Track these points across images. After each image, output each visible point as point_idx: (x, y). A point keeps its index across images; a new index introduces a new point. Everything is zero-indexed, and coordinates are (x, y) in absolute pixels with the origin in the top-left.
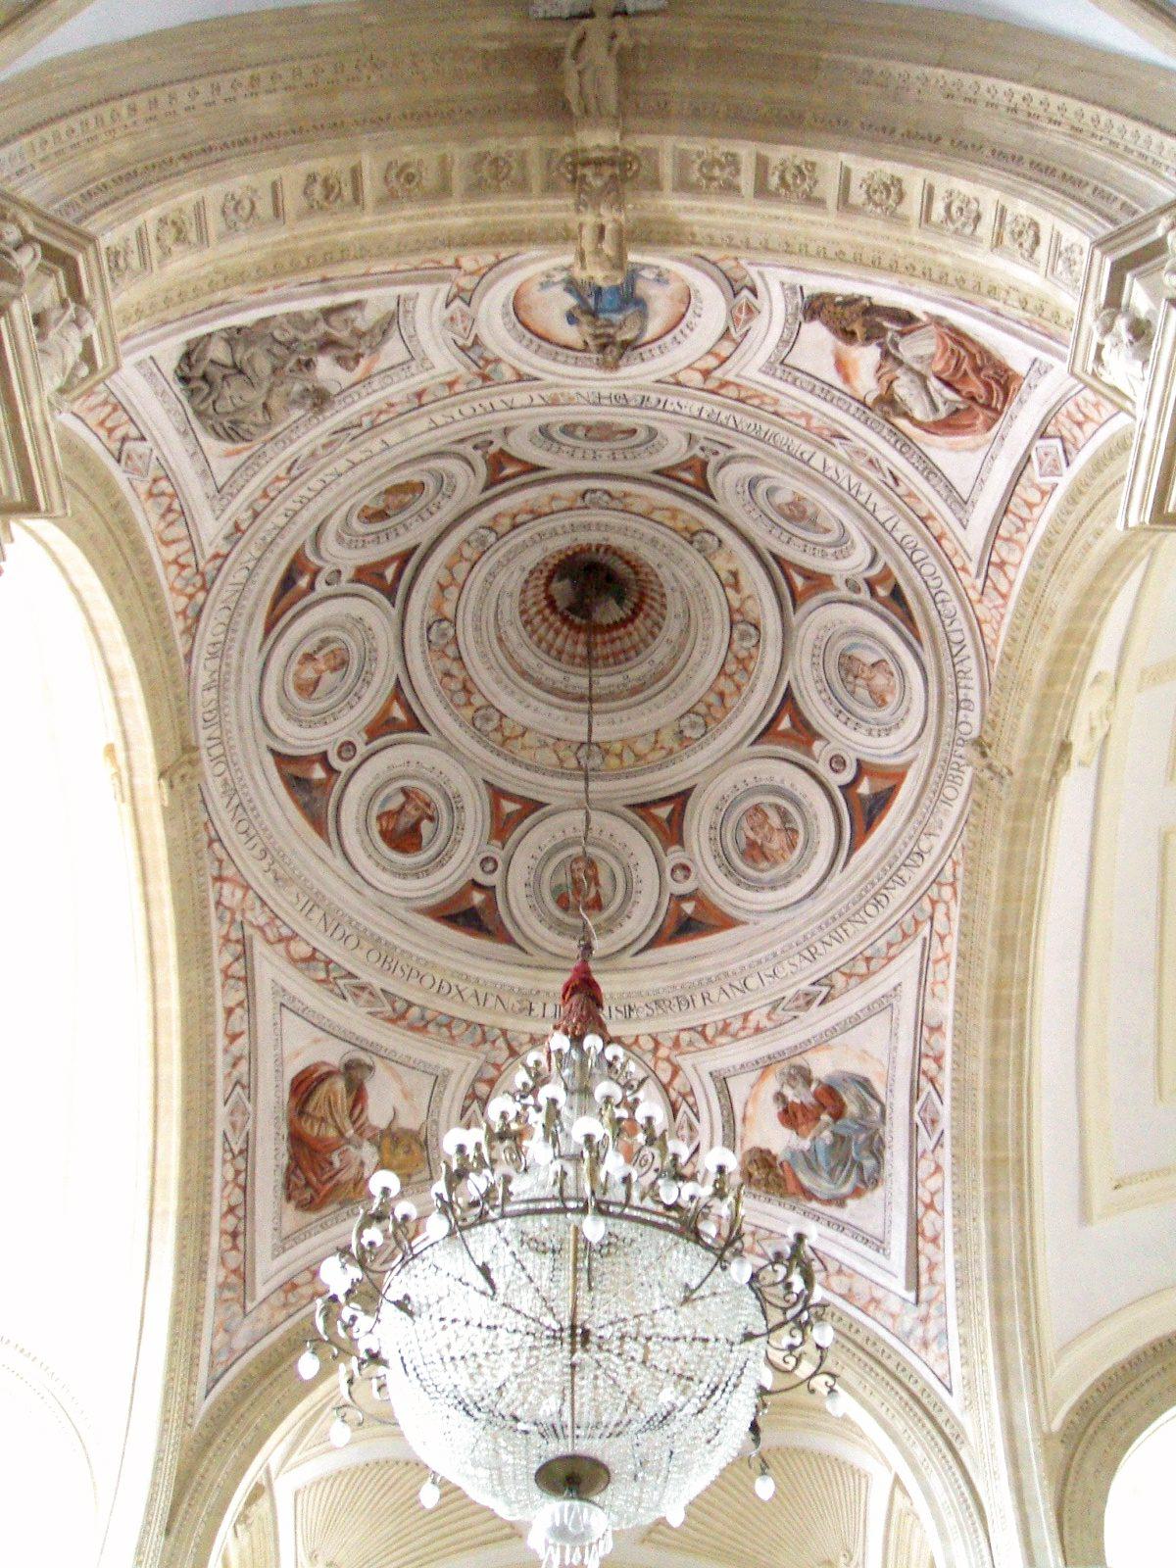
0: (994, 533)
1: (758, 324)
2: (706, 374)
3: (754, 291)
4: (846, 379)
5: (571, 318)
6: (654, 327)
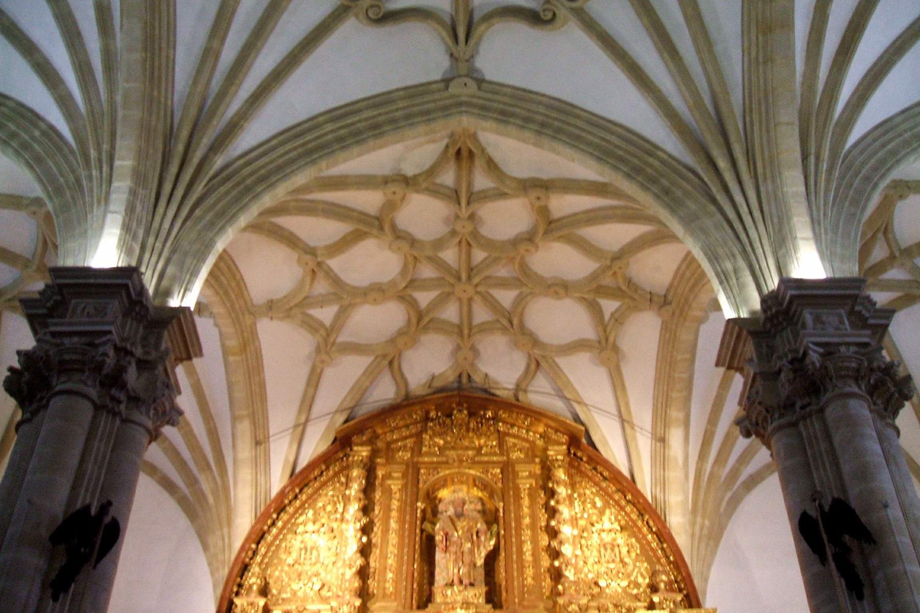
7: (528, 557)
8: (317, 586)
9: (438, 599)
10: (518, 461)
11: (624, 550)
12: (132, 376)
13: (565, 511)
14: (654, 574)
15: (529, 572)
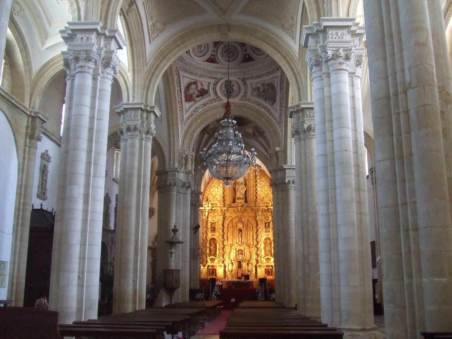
0: (179, 77)
1: (213, 87)
2: (217, 79)
3: (214, 92)
4: (201, 83)
5: (233, 85)
6: (224, 83)
8: (216, 199)
9: (236, 202)
11: (269, 191)
12: (197, 205)
13: (258, 185)
15: (252, 196)
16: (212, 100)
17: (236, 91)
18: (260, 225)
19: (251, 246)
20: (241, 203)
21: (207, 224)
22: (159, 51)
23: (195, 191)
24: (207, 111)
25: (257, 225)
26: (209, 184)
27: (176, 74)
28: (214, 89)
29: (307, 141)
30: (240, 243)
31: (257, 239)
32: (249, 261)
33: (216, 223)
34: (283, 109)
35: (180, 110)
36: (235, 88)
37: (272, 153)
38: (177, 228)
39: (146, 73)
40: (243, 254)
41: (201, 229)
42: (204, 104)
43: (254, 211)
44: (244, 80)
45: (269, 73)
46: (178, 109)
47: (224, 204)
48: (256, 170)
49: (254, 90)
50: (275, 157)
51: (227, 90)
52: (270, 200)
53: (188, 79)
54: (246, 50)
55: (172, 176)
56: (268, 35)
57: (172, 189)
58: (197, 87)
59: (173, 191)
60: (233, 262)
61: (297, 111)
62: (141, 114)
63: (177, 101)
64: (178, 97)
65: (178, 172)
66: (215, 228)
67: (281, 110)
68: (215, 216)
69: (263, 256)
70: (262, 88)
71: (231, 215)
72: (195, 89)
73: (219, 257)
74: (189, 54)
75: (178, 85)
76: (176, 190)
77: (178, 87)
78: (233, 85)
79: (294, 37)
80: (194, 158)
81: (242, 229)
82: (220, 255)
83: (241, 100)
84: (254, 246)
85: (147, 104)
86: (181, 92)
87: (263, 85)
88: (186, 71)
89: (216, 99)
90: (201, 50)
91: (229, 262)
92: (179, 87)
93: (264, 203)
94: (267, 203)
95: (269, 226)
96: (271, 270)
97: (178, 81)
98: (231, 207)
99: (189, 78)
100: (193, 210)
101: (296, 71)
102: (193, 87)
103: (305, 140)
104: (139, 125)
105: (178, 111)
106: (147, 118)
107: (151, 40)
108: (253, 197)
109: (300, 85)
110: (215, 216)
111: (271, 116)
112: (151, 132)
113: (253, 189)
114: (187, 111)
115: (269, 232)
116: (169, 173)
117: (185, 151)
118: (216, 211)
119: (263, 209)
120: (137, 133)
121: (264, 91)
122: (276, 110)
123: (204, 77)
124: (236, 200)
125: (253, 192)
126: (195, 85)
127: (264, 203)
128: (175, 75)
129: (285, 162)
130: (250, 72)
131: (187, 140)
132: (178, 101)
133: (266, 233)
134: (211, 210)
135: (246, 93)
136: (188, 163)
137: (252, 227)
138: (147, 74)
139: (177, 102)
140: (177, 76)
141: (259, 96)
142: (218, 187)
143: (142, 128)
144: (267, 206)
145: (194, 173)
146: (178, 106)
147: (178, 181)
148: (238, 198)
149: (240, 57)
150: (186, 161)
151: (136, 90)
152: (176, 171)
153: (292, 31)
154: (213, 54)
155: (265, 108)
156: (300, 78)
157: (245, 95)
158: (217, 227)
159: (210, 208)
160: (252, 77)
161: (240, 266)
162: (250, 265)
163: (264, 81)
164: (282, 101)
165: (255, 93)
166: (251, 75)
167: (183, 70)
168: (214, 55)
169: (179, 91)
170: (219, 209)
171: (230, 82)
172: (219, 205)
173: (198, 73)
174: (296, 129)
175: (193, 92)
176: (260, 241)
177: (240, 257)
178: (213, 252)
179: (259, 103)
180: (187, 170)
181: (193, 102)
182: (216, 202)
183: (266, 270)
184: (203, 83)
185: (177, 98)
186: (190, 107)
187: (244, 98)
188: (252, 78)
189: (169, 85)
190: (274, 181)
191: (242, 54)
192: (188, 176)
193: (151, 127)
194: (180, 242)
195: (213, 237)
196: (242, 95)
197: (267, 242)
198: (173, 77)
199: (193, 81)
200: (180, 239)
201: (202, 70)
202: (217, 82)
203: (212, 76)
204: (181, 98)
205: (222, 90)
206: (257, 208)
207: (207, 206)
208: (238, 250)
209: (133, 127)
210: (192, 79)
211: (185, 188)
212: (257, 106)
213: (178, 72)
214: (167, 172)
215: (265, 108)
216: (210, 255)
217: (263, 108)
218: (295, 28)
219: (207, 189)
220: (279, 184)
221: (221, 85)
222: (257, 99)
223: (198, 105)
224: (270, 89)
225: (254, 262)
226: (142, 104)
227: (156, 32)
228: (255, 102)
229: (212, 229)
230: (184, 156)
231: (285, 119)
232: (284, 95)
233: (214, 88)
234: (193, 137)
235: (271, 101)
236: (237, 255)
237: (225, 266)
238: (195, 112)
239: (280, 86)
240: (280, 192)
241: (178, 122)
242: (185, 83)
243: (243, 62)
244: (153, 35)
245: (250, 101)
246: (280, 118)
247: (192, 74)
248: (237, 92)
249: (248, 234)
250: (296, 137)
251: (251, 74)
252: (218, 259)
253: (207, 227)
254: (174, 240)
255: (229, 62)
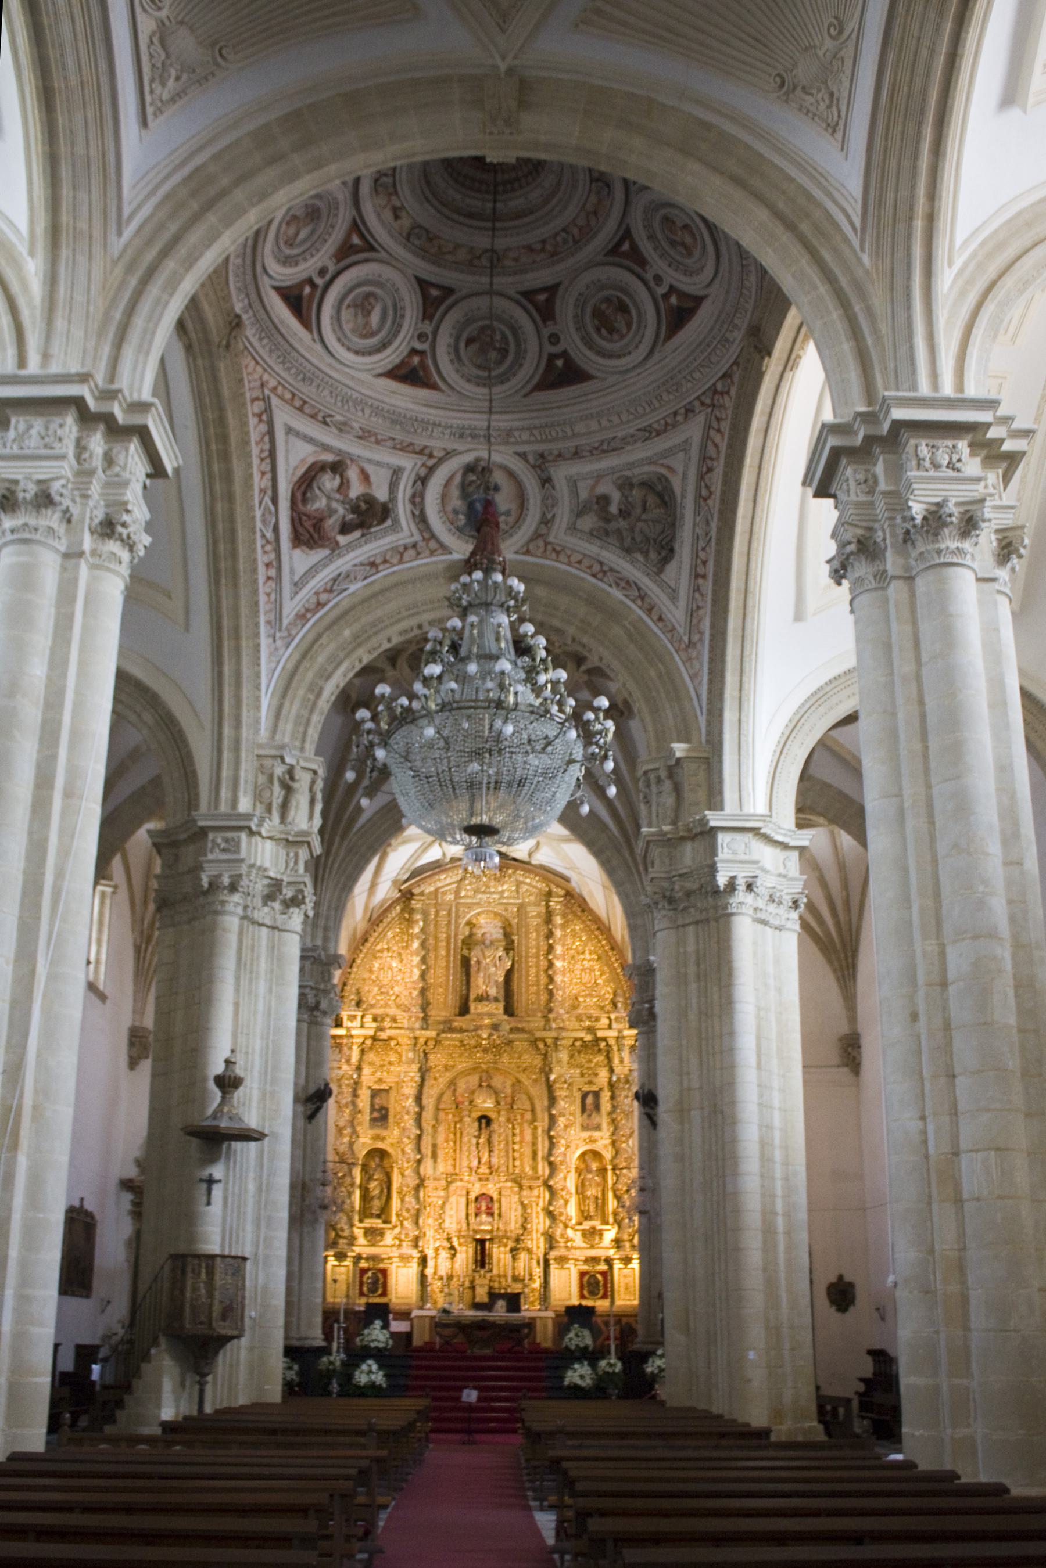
0: (271, 433)
1: (409, 492)
2: (431, 456)
3: (413, 514)
5: (497, 489)
6: (458, 479)
7: (532, 978)
10: (529, 904)
11: (598, 973)
12: (324, 1005)
13: (559, 950)
14: (615, 994)
16: (406, 548)
17: (508, 513)
18: (562, 1103)
19: (525, 1183)
20: (490, 1015)
21: (355, 1095)
22: (186, 170)
23: (315, 948)
24: (382, 592)
25: (552, 1100)
26: (366, 940)
27: (259, 416)
28: (417, 500)
29: (920, 583)
30: (484, 1169)
31: (550, 1153)
32: (517, 1240)
33: (393, 1094)
34: (708, 586)
35: (269, 578)
36: (504, 501)
37: (657, 769)
38: (239, 1071)
39: (115, 262)
40: (496, 1212)
41: (331, 1101)
42: (373, 564)
43: (541, 1045)
44: (541, 464)
45: (649, 433)
46: (261, 569)
47: (425, 1019)
48: (549, 894)
49: (581, 512)
50: (667, 785)
51: (471, 506)
52: (602, 1008)
53: (309, 448)
54: (554, 339)
55: (224, 850)
56: (707, 126)
57: (223, 903)
58: (344, 485)
59: (223, 913)
60: (456, 1243)
61: (862, 453)
62: (78, 441)
63: (258, 535)
64: (264, 522)
65: (251, 833)
66: (387, 1110)
67: (697, 589)
68: (390, 1063)
69: (574, 1222)
70: (616, 496)
71: (451, 1063)
72: (338, 496)
73: (402, 1224)
74: (316, 337)
75: (266, 466)
76: (240, 910)
77: (263, 474)
78: (497, 489)
79: (842, 123)
80: (320, 784)
81: (493, 1115)
82: (405, 1214)
83: (528, 552)
84: (540, 1182)
85: (115, 386)
86: (275, 500)
87: (625, 485)
88: (300, 409)
89: (421, 544)
90: (367, 324)
91: (437, 1244)
92: (269, 476)
93: (579, 1019)
94: (589, 1018)
95: (597, 1107)
96: (604, 1274)
97: (267, 447)
98: (451, 1030)
99: (310, 440)
100: (305, 1026)
101: (844, 281)
102: (329, 482)
103: (910, 579)
104: (63, 482)
105: (261, 579)
106: (109, 460)
107: (150, 110)
108: (537, 993)
109: (869, 341)
110: (390, 1063)
111: (649, 616)
112: (124, 525)
113: (538, 966)
114: (298, 586)
115: (598, 1128)
116: (211, 836)
117: (282, 747)
118: (393, 1043)
119: (576, 1040)
120: (52, 519)
121: (624, 513)
122: (673, 596)
123: (378, 442)
124: (472, 1006)
125: (537, 976)
126: (338, 478)
127: (579, 1019)
128: (256, 420)
129: (714, 799)
130: (568, 430)
131: (293, 708)
132: (263, 536)
133: (586, 1134)
134: (374, 1038)
135: (546, 522)
136: (293, 803)
137: (533, 1110)
138: (119, 270)
139: (259, 542)
140: (263, 428)
141: (600, 534)
142: (400, 954)
143: (78, 499)
144: (591, 1030)
145: (318, 849)
146: (261, 559)
147: (249, 874)
148: (480, 999)
149: (530, 369)
150: (288, 790)
151: (60, 324)
152: (240, 829)
153: (832, 95)
154: (419, 346)
155: (626, 584)
156: (869, 311)
157: (543, 530)
158: (393, 1107)
159: (371, 1033)
160: (576, 453)
161: (482, 1259)
162: (523, 1256)
163: (631, 465)
164: (702, 554)
165: (588, 522)
166: (571, 444)
167: (290, 402)
168: (421, 353)
169: (269, 493)
170: (404, 1037)
171: (486, 471)
172: (404, 1021)
173: (356, 425)
174: (860, 532)
175: (328, 505)
176: (561, 1163)
177: (485, 1225)
178: (377, 1204)
179: (601, 563)
180: (289, 827)
181: (327, 552)
182: (392, 1011)
183: (582, 1274)
184: (370, 469)
185: (259, 524)
186: (312, 571)
187: (541, 543)
188: (577, 454)
189: (225, 457)
190: (666, 885)
191: (540, 356)
192: (292, 854)
193: (126, 503)
194: (248, 1136)
195: (379, 1145)
196: (530, 533)
197: (589, 1170)
198: (244, 424)
199: (329, 457)
200: (252, 1120)
201: (367, 411)
202: (431, 470)
203: (409, 439)
204: (276, 529)
205: (449, 508)
206: (554, 1034)
207: (357, 1023)
208: (477, 1199)
209: (32, 489)
210: (326, 448)
211: (277, 905)
212: (594, 576)
213: (268, 410)
214: (204, 832)
215: (626, 584)
216: (365, 1214)
217: (618, 585)
218: (848, 72)
219: (358, 961)
220: (689, 894)
221: (447, 485)
222: (592, 548)
223: (344, 563)
224: (651, 500)
225: (537, 1244)
226: (84, 378)
227: (173, 73)
228: (586, 562)
229: (376, 1115)
230: (279, 770)
231: (713, 626)
232: (714, 525)
233: (414, 496)
234: (319, 695)
235: (653, 555)
236: (472, 1219)
237: (423, 1261)
238: (331, 591)
239: (698, 489)
240: (691, 929)
241: (257, 625)
242: (294, 461)
243: (540, 387)
244: (158, 89)
245: (562, 557)
246: (693, 627)
247: (325, 423)
248: (511, 519)
249: (514, 1135)
250: (861, 569)
251: (575, 435)
252: (397, 1230)
253: (354, 1103)
254: (224, 1123)
255: (479, 382)
